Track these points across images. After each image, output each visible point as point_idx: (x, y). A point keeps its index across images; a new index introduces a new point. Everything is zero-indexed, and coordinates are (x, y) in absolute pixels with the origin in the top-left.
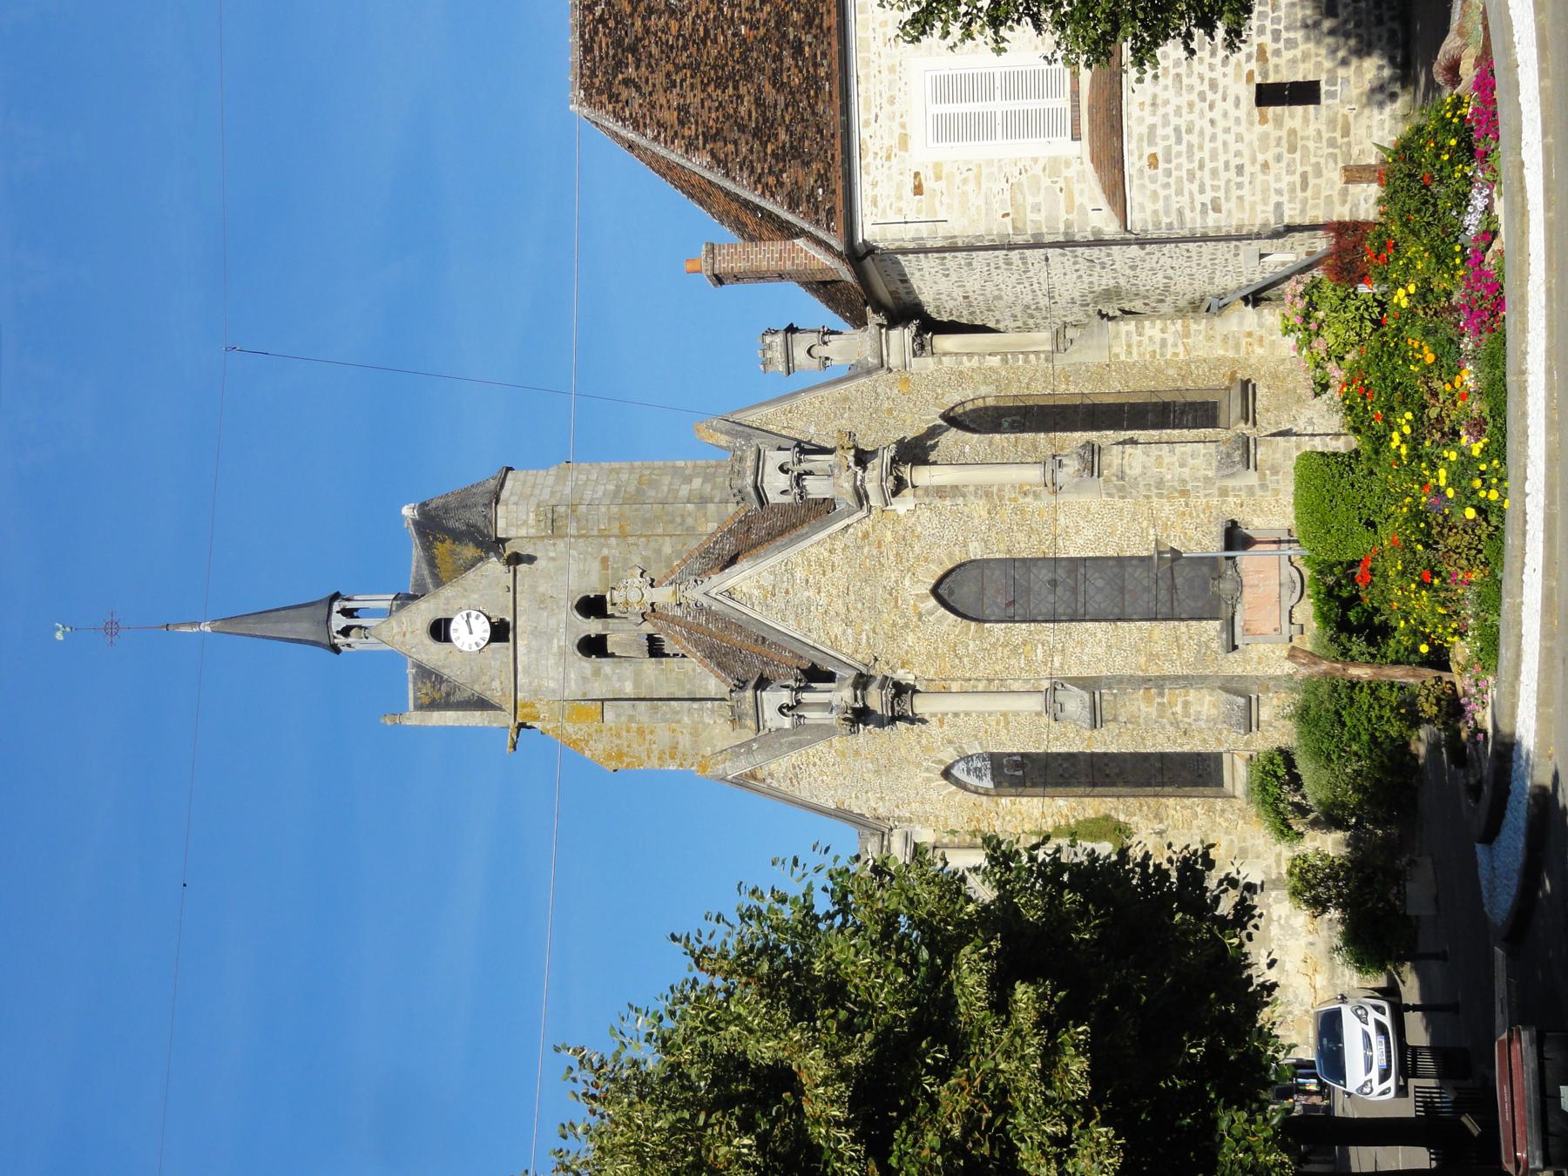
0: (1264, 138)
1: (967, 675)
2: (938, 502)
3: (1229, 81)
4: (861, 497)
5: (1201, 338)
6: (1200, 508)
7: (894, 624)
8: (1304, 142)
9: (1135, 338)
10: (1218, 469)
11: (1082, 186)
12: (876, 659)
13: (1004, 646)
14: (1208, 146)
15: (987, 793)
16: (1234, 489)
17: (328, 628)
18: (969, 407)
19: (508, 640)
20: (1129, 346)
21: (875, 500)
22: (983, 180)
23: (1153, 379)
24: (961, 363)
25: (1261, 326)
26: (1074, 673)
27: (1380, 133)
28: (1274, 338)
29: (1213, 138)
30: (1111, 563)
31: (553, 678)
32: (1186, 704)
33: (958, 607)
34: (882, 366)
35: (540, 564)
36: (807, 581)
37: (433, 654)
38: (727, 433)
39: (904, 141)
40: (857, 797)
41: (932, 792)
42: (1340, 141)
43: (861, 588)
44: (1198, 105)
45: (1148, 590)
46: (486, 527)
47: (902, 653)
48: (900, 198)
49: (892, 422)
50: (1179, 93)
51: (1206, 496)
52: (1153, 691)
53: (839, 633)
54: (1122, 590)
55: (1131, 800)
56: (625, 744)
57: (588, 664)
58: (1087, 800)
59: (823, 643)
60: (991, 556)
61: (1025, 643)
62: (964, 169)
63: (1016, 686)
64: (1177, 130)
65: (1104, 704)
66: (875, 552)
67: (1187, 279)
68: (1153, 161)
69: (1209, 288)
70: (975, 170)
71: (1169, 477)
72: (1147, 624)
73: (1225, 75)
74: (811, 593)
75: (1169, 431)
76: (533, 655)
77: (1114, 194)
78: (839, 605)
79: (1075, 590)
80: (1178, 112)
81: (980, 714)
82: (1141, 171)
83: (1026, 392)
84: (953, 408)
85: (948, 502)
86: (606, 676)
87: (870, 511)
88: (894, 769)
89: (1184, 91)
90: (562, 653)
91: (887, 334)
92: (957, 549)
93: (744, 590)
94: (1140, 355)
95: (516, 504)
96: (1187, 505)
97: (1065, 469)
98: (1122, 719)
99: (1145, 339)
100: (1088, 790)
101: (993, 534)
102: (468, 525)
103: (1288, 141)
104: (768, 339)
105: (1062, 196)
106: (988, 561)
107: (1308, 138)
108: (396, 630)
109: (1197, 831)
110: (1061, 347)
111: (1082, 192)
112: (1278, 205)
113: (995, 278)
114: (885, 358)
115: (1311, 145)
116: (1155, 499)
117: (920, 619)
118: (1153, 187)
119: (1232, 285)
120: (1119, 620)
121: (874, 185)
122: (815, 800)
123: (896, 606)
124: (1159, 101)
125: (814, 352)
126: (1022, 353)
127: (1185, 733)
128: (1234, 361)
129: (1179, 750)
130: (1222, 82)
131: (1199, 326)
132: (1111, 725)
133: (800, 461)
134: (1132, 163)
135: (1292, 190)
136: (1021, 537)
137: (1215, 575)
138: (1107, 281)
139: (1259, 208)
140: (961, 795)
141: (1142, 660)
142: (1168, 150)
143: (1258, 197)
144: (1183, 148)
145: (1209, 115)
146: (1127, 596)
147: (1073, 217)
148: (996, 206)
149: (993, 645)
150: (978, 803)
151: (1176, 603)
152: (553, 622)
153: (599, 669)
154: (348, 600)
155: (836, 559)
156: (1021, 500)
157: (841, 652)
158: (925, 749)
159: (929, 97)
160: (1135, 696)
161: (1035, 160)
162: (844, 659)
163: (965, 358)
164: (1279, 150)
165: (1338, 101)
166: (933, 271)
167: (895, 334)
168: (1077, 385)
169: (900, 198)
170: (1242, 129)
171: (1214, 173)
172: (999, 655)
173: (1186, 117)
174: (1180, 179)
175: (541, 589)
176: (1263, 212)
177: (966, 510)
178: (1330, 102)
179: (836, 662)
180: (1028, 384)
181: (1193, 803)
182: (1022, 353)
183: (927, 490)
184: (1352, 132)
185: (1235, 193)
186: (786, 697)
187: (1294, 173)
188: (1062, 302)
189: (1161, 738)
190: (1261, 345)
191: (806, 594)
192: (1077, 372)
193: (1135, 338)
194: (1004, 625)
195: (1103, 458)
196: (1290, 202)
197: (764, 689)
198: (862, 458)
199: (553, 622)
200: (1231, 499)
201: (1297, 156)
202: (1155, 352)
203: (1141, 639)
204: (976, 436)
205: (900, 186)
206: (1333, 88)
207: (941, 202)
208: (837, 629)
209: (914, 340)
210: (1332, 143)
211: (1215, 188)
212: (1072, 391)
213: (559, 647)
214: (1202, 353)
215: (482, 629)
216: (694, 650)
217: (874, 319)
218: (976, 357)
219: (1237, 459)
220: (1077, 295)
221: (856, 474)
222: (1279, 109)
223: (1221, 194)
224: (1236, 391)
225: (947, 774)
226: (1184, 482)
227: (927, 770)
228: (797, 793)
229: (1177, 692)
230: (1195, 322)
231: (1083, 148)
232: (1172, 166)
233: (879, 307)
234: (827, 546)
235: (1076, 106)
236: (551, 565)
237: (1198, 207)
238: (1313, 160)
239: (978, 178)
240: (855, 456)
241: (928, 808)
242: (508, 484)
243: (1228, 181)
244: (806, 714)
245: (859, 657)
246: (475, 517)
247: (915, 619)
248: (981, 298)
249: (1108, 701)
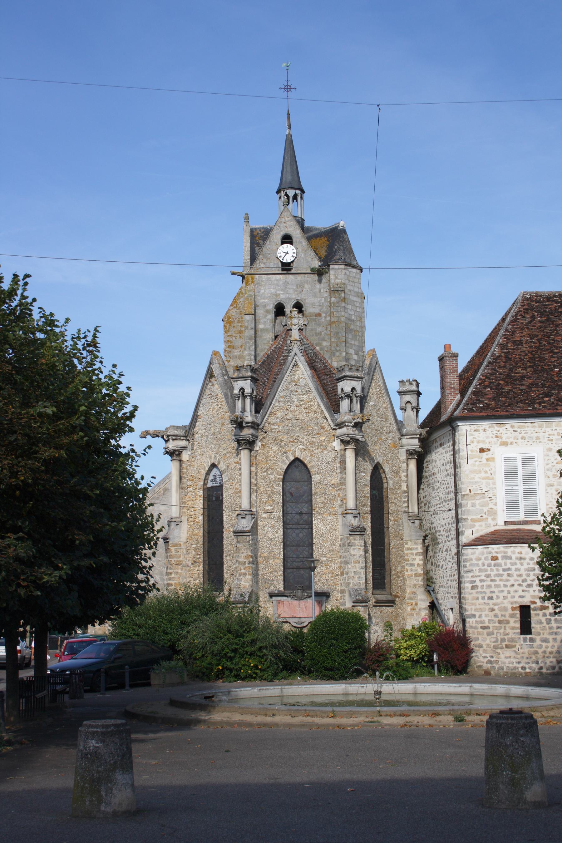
0: (505, 609)
1: (258, 475)
2: (338, 460)
3: (532, 593)
4: (340, 425)
5: (415, 582)
6: (335, 581)
7: (282, 441)
8: (503, 627)
9: (414, 552)
10: (353, 589)
11: (484, 526)
12: (266, 432)
13: (272, 491)
14: (502, 583)
15: (205, 484)
16: (344, 596)
17: (288, 188)
18: (383, 475)
19: (282, 271)
20: (411, 549)
21: (339, 432)
22: (487, 480)
23: (396, 560)
24: (403, 472)
25: (420, 609)
26: (260, 523)
27: (507, 662)
28: (415, 615)
29: (505, 586)
30: (310, 540)
31: (265, 291)
32: (245, 574)
33: (290, 471)
34: (402, 435)
35: (318, 286)
36: (301, 401)
37: (276, 236)
38: (371, 364)
39: (505, 444)
40: (203, 424)
41: (205, 459)
42: (504, 644)
43: (298, 425)
44: (520, 579)
45: (298, 557)
46: (335, 260)
47: (269, 445)
48: (478, 442)
49: (376, 440)
50: (526, 570)
51: (341, 584)
52: (251, 559)
53: (277, 416)
54: (298, 545)
55: (202, 550)
56: (235, 325)
57: (271, 307)
58: (202, 530)
59: (273, 408)
60: (313, 485)
61: (273, 501)
62: (492, 472)
63: (254, 497)
64: (509, 569)
65: (245, 537)
66: (315, 432)
67: (442, 575)
68: (495, 558)
69: (438, 585)
70: (491, 477)
71: (350, 567)
72: (282, 556)
73: (534, 591)
74: (296, 403)
75: (371, 567)
76: (275, 282)
77: (479, 540)
78: (290, 415)
79: (298, 524)
80: (517, 570)
81: (240, 480)
82: (490, 553)
83: (390, 502)
84: (382, 468)
85: (338, 465)
86: (266, 316)
87: (334, 429)
88: (215, 442)
89: (526, 572)
90: (277, 295)
91: (416, 438)
92: (316, 469)
93: (298, 372)
94: (407, 554)
95: (345, 274)
96: (337, 575)
97: (353, 519)
98: (238, 545)
99: (414, 556)
100: (206, 530)
101: (323, 486)
102: (336, 252)
103: (503, 620)
104: (414, 383)
105: (479, 517)
106: (311, 484)
107: (505, 629)
108: (287, 219)
109: (188, 581)
110: (410, 518)
111: (481, 526)
112: (474, 616)
113: (442, 487)
114: (406, 437)
115: (502, 631)
116: (339, 560)
117: (284, 452)
118: (483, 558)
119: (439, 596)
120: (284, 544)
121: (484, 430)
122: (201, 405)
123: (290, 442)
124: (522, 561)
125: (409, 405)
126: (408, 500)
127: (232, 574)
128: (404, 597)
129: (225, 572)
130: (531, 590)
131: (420, 581)
132: (235, 540)
133: (356, 397)
134: (493, 549)
135: (482, 622)
136: (322, 499)
137: (304, 588)
138: (441, 539)
139: (473, 607)
140: (204, 472)
141: (265, 555)
142: (500, 565)
143: (478, 607)
144: (501, 572)
145: (516, 584)
146: (295, 548)
147: (470, 522)
148: (474, 486)
149: (272, 486)
150: (200, 480)
151: (291, 570)
152: (291, 291)
154: (301, 197)
155: (312, 414)
156: (339, 499)
157: (269, 416)
158: (224, 455)
159: (524, 455)
160: (248, 551)
161: (495, 505)
162: (266, 418)
163: (405, 474)
164: (500, 616)
165: (522, 643)
166: (445, 458)
167: (417, 441)
168: (393, 525)
169: (478, 442)
170: (509, 599)
171: (489, 586)
172: (268, 489)
173: (515, 573)
174: (486, 570)
175: (306, 286)
176: (471, 609)
177: (334, 474)
178: (522, 639)
179: (264, 414)
180: (393, 503)
181: (201, 578)
182: (408, 500)
183: (343, 456)
184: (508, 650)
185: (480, 596)
186: (248, 391)
187: (489, 623)
188: (432, 519)
189: (230, 563)
190: (411, 609)
191: (296, 400)
192: (399, 525)
193: (414, 552)
194: (281, 491)
195: (358, 536)
196: (476, 621)
197: (251, 381)
198: (358, 425)
200: (340, 595)
201: (497, 624)
202: (409, 561)
203: (275, 554)
204: (369, 478)
205: (484, 442)
206: (528, 640)
207: (476, 461)
208: (279, 415)
209: (414, 450)
210: (503, 640)
211: (482, 587)
212: (390, 523)
213: (279, 294)
214: (408, 582)
215: (288, 259)
216: (271, 350)
217: (424, 431)
218: (406, 479)
219: (358, 598)
220: (435, 525)
221: (351, 423)
222: (518, 616)
223: (480, 590)
224: (390, 598)
225: (213, 466)
226: (347, 573)
227: (215, 456)
228: (205, 397)
229: (251, 570)
230: (422, 579)
231: (501, 526)
232: (493, 567)
233: (429, 434)
234: (318, 410)
235: (520, 523)
236: (317, 290)
237: (474, 579)
238: (495, 632)
239: (487, 478)
240: (359, 422)
241: (198, 457)
242: (354, 270)
243: (485, 593)
244: (240, 401)
245: (267, 425)
246: (340, 255)
247: (284, 450)
248: (433, 481)
249: (246, 539)
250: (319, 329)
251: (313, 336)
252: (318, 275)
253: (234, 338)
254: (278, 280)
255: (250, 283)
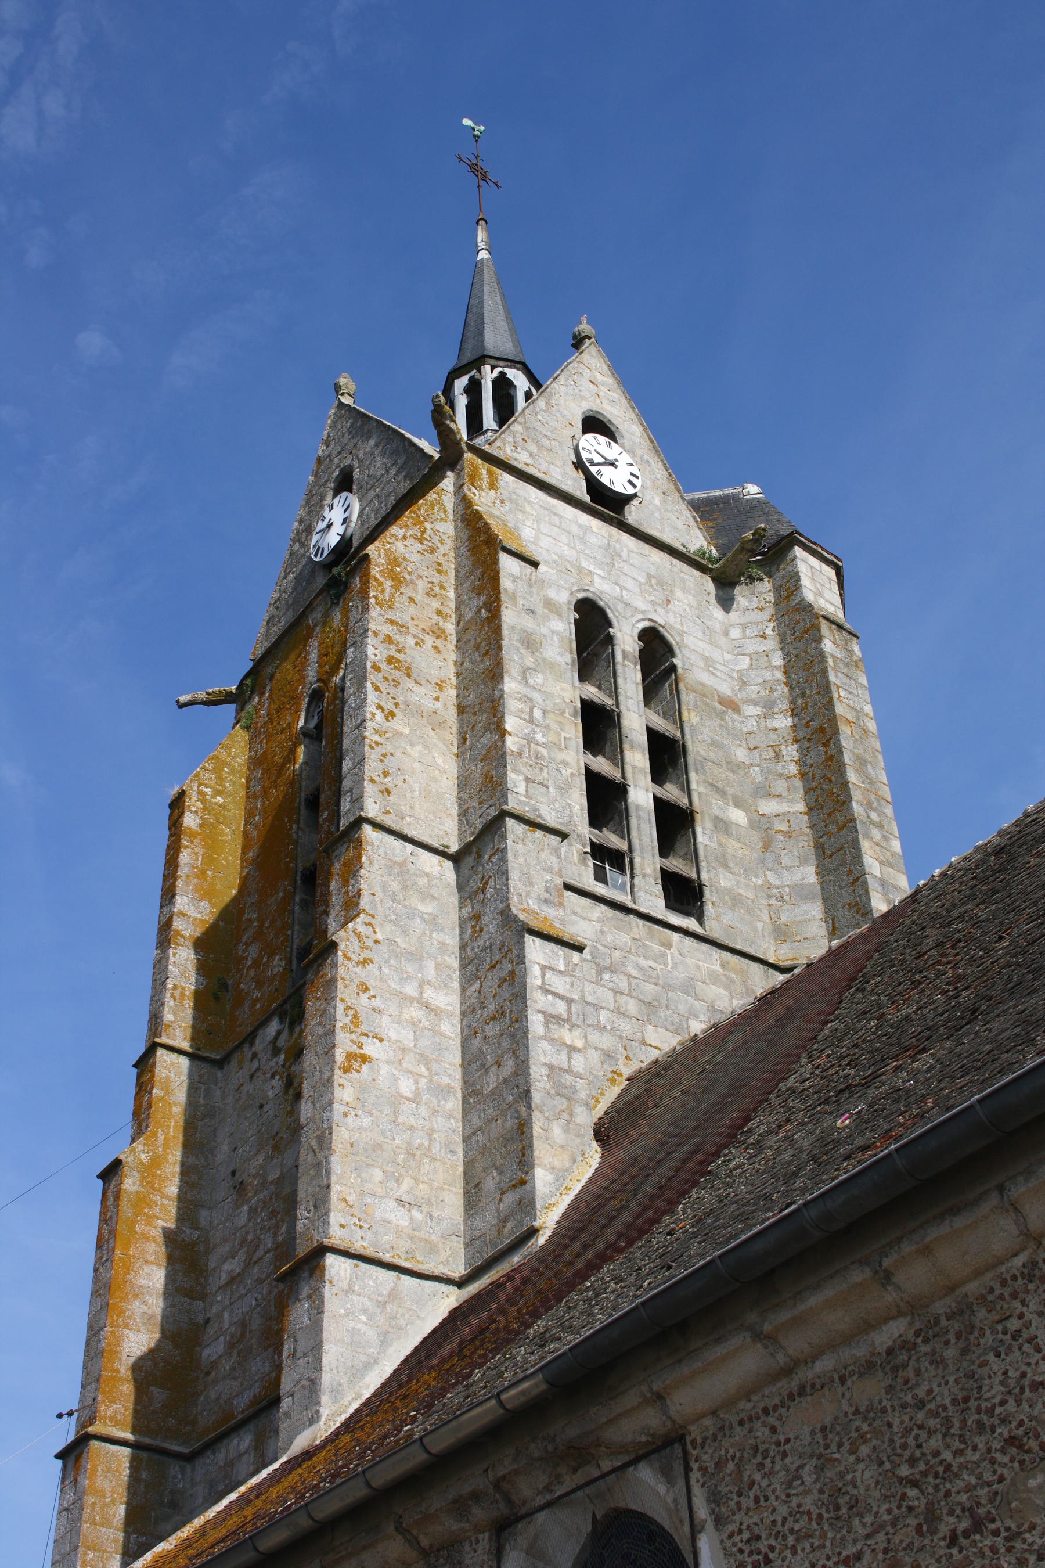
17: (513, 363)
35: (718, 613)
153: (560, 615)
199: (630, 584)
236: (717, 627)
250: (741, 754)
251: (719, 765)
252: (713, 579)
253: (412, 642)
254: (586, 529)
255: (485, 485)
